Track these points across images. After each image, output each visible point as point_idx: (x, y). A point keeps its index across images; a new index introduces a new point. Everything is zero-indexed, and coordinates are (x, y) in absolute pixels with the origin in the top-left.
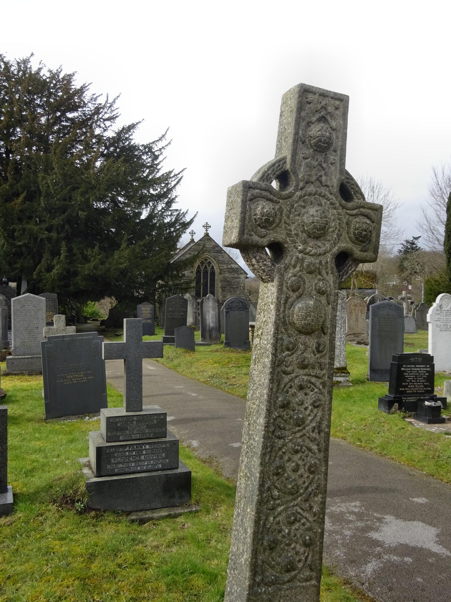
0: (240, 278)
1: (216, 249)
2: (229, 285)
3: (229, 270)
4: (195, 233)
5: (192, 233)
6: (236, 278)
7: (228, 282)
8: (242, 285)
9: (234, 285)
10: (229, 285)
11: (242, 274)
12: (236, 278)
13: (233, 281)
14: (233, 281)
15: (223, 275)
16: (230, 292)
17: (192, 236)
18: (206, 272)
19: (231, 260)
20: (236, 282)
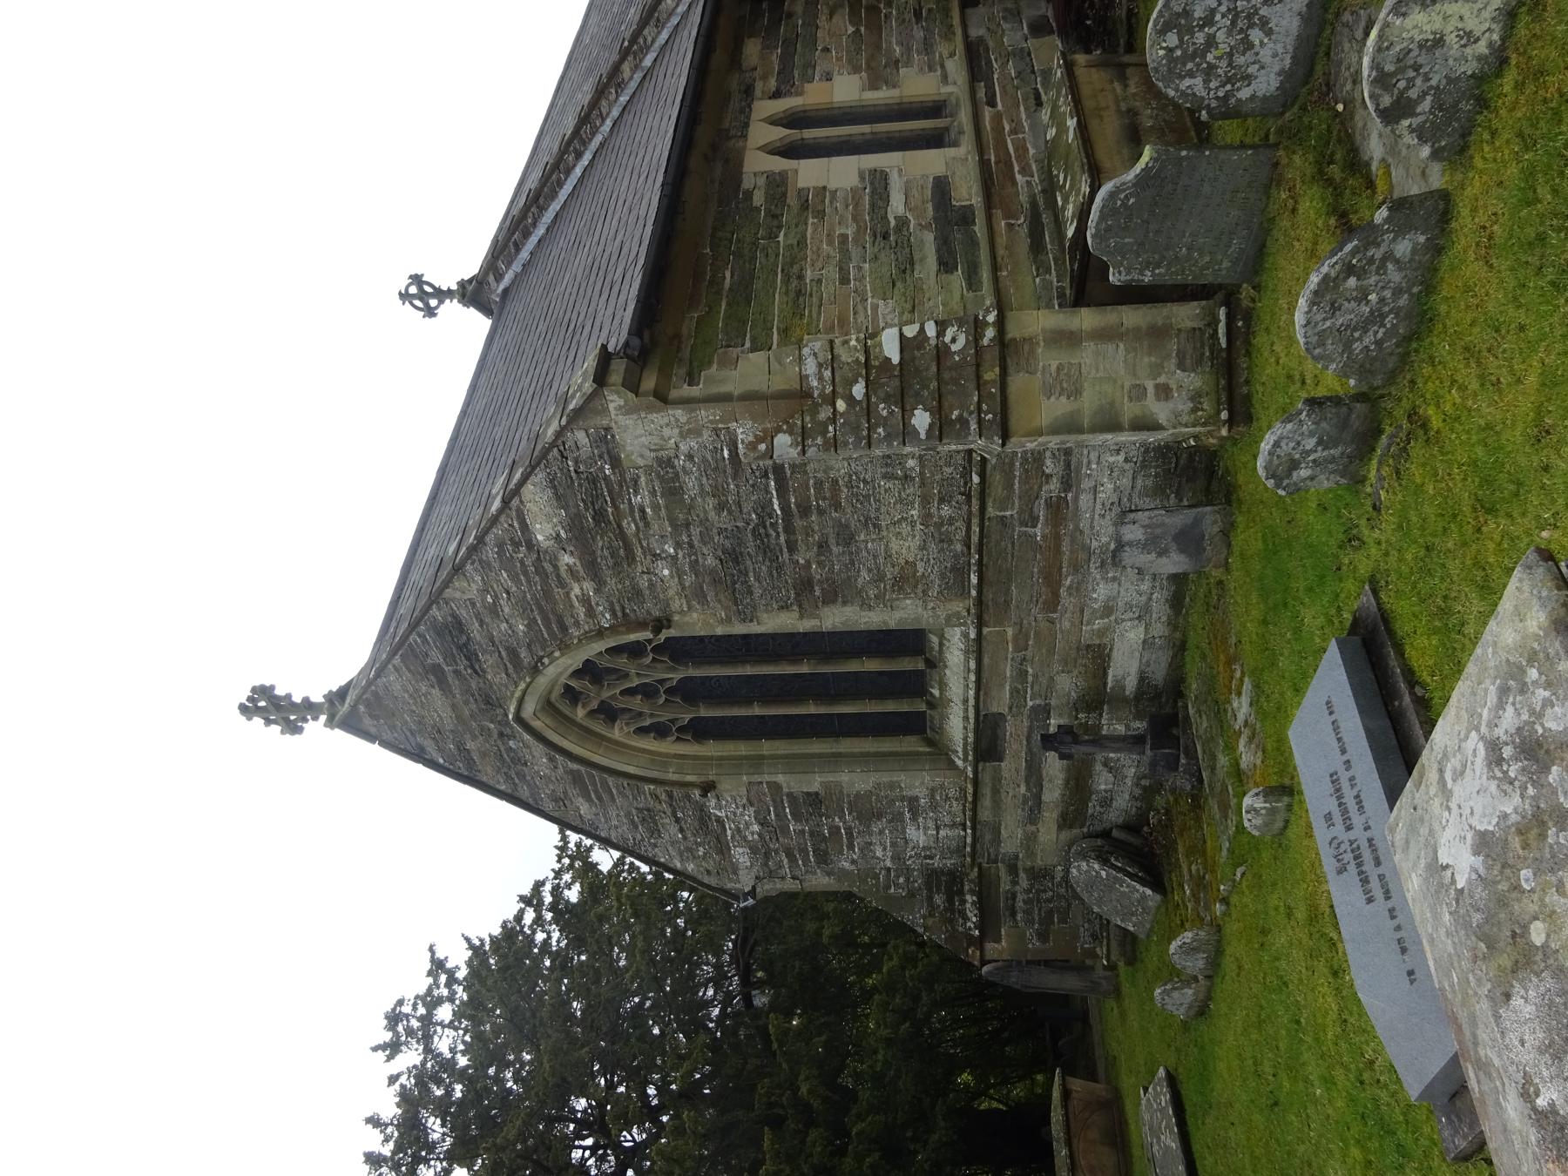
0: (667, 463)
1: (436, 657)
2: (769, 552)
3: (605, 562)
4: (417, 279)
5: (423, 296)
6: (673, 491)
7: (733, 557)
8: (744, 432)
9: (764, 508)
10: (769, 552)
11: (606, 443)
12: (673, 491)
13: (723, 521)
14: (723, 521)
15: (676, 604)
16: (847, 537)
17: (442, 295)
18: (688, 692)
19: (490, 553)
20: (718, 491)
